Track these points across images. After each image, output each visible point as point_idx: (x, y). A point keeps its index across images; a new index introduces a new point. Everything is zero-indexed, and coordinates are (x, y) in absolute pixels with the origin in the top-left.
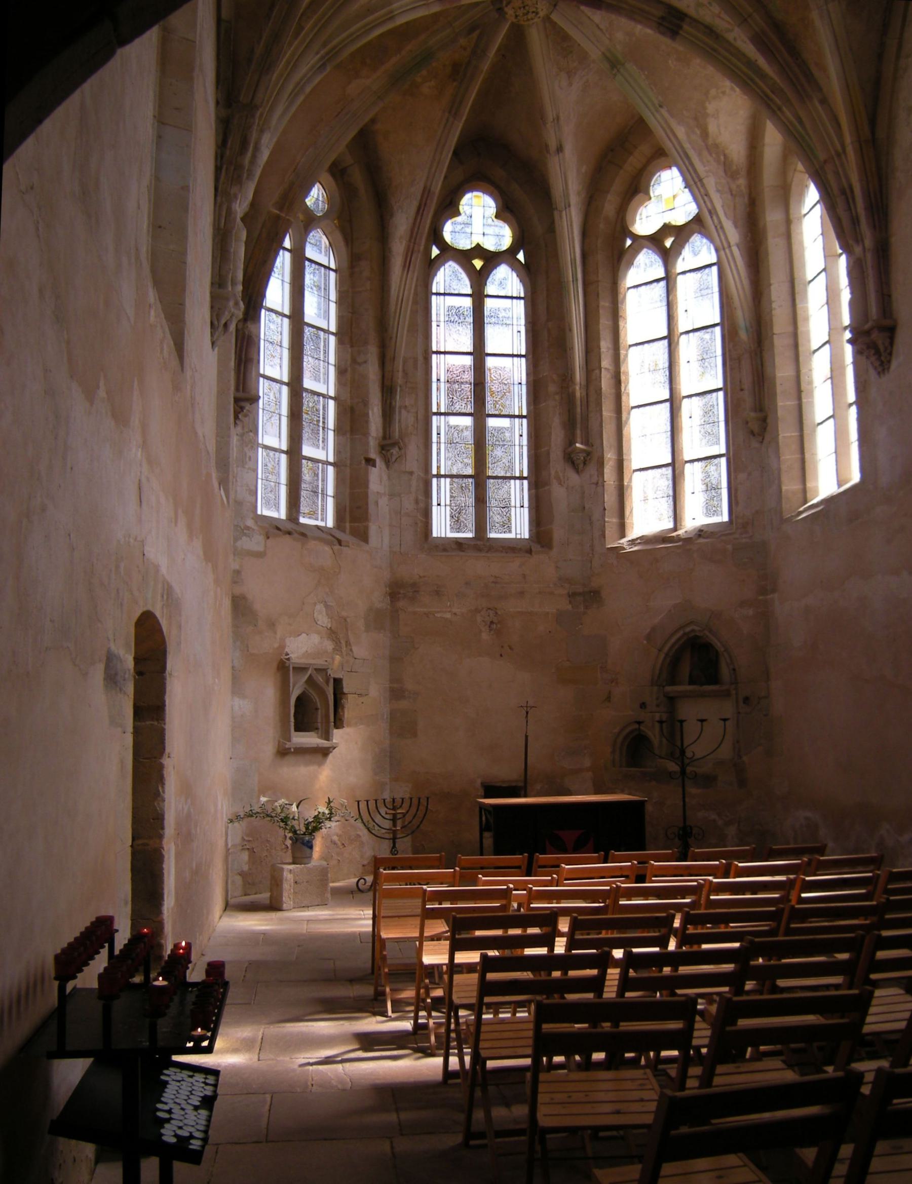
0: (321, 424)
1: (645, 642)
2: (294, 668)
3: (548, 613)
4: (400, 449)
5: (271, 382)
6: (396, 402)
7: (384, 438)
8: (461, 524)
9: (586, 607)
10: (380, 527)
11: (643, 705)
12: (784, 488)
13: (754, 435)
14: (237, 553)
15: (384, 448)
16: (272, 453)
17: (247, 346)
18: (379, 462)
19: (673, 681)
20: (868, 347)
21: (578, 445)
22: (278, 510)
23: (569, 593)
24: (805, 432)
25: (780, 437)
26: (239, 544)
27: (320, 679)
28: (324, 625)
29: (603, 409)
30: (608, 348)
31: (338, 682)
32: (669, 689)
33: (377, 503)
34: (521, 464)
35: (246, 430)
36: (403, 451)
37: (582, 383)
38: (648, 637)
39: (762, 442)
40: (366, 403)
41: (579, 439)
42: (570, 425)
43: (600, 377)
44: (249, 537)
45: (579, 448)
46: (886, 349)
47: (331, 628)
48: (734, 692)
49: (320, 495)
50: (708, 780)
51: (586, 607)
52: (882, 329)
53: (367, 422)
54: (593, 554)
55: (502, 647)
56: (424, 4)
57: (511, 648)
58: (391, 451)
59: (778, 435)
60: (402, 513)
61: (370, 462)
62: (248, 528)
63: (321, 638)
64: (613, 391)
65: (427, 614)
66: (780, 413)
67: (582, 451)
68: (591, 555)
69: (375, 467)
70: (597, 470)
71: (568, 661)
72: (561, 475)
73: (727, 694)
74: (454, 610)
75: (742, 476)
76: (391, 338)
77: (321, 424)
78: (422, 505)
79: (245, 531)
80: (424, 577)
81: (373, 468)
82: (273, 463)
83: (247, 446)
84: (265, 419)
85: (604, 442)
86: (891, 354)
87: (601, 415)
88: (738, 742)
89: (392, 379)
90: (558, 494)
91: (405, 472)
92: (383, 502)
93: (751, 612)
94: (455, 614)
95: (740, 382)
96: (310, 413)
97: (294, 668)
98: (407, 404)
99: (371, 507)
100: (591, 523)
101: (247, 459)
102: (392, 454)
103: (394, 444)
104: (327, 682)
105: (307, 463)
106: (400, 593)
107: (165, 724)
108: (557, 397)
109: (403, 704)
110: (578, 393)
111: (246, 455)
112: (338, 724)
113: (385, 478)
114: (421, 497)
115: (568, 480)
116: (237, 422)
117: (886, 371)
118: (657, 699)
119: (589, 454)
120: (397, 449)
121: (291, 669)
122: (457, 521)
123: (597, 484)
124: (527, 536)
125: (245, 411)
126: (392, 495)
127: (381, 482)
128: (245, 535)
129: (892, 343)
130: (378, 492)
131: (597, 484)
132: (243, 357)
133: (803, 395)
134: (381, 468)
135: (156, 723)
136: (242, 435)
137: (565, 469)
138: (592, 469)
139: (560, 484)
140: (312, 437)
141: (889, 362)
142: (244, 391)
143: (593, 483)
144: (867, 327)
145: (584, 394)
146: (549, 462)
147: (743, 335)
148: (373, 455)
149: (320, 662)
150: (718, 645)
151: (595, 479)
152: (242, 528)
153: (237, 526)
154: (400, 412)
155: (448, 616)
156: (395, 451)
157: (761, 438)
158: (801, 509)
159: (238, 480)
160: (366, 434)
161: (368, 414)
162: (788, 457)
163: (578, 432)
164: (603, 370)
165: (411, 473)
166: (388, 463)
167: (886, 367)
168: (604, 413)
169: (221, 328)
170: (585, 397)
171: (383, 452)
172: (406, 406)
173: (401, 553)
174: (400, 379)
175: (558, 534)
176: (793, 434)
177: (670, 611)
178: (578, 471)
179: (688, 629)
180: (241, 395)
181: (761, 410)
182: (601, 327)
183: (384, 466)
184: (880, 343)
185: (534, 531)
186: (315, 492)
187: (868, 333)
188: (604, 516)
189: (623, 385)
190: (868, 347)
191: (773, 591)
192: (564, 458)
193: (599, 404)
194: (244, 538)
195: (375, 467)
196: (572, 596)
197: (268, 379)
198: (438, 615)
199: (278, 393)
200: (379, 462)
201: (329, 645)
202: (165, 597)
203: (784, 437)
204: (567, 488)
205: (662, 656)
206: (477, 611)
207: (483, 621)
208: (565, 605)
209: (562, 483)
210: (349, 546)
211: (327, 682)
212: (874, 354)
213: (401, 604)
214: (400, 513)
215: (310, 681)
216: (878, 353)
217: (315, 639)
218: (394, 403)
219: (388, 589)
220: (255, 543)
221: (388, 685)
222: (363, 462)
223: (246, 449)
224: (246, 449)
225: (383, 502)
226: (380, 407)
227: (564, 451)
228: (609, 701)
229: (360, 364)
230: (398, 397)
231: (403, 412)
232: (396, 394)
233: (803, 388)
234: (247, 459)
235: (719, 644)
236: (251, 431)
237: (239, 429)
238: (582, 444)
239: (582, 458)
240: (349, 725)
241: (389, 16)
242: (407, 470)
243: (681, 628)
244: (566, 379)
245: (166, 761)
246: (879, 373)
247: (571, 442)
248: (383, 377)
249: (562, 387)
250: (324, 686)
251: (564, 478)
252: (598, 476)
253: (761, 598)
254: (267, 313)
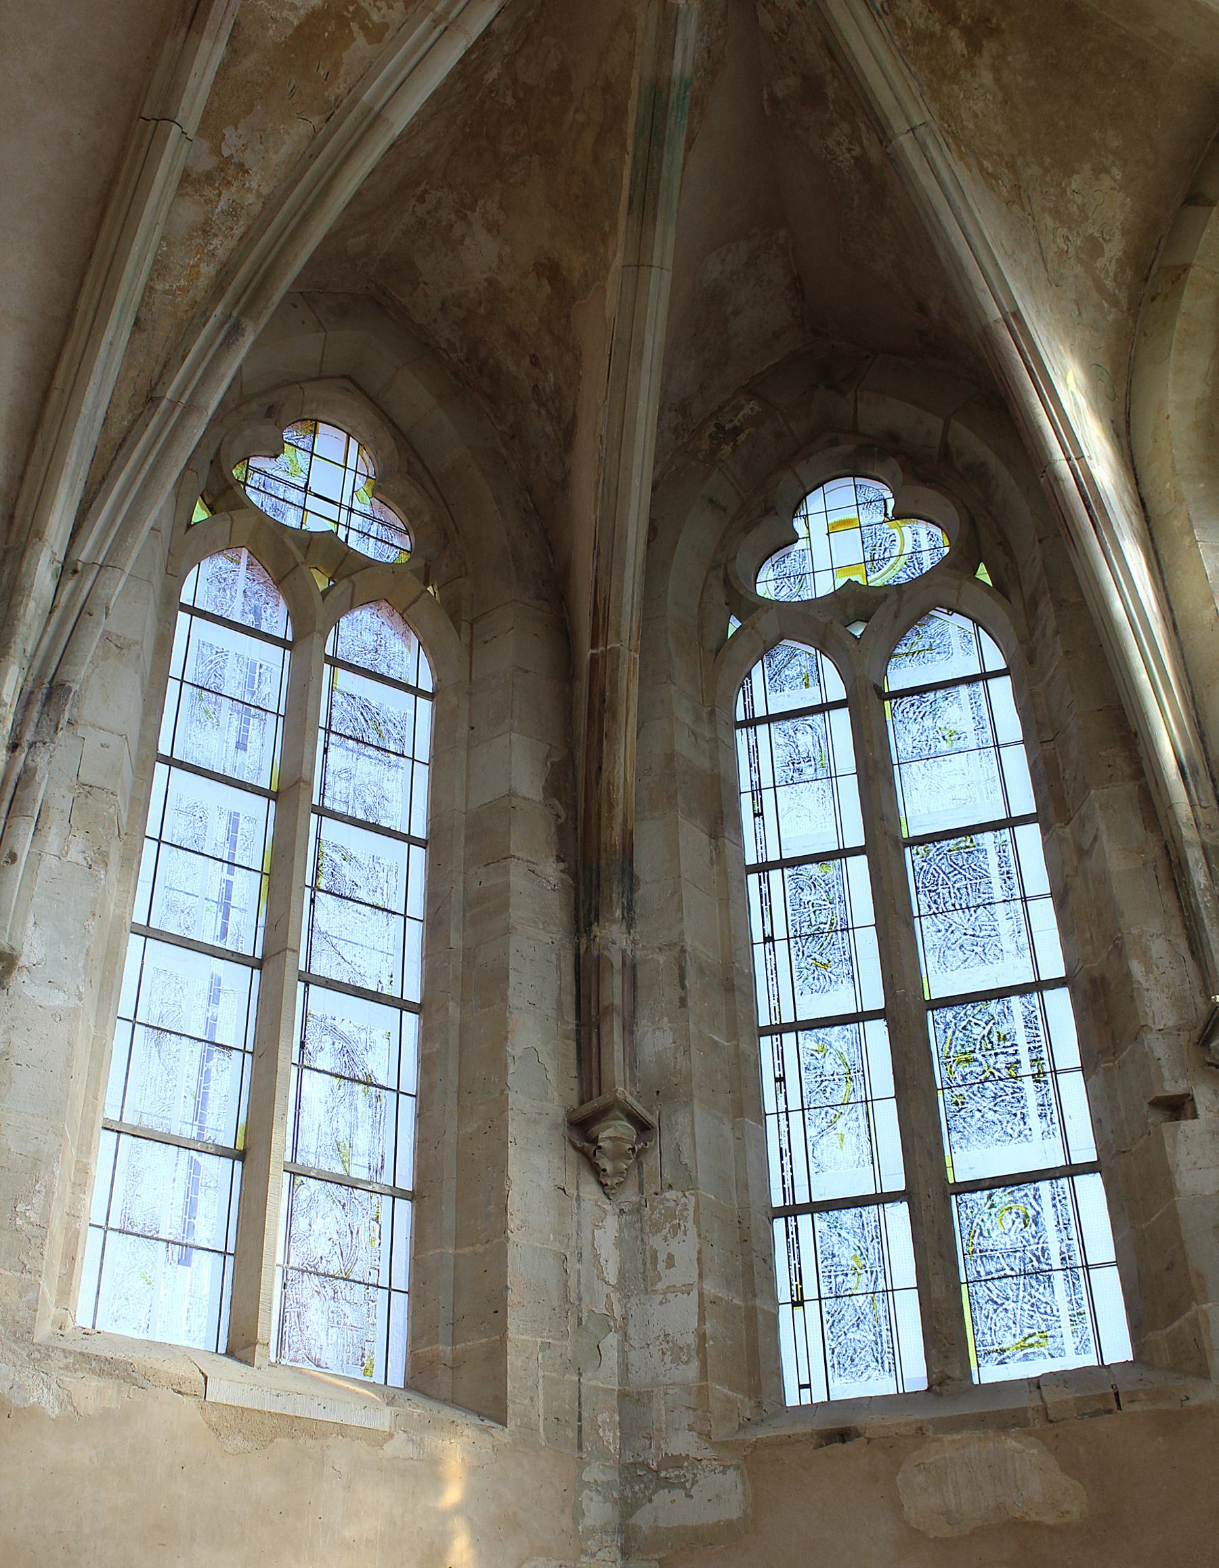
0: (1026, 1069)
5: (821, 1033)
16: (847, 1217)
18: (1203, 1096)
22: (895, 1367)
26: (643, 1519)
35: (650, 1189)
44: (682, 1486)
49: (1058, 1277)
56: (446, 29)
62: (676, 1461)
77: (1026, 1069)
79: (663, 1474)
82: (854, 1242)
83: (659, 1231)
84: (811, 1132)
96: (978, 1055)
105: (990, 1197)
128: (667, 1484)
140: (995, 1117)
152: (654, 1467)
159: (631, 1331)
197: (810, 1029)
199: (854, 1050)
223: (655, 1241)
224: (655, 1241)
234: (661, 1266)
236: (670, 1187)
237: (629, 1195)
241: (370, 118)
254: (787, 872)
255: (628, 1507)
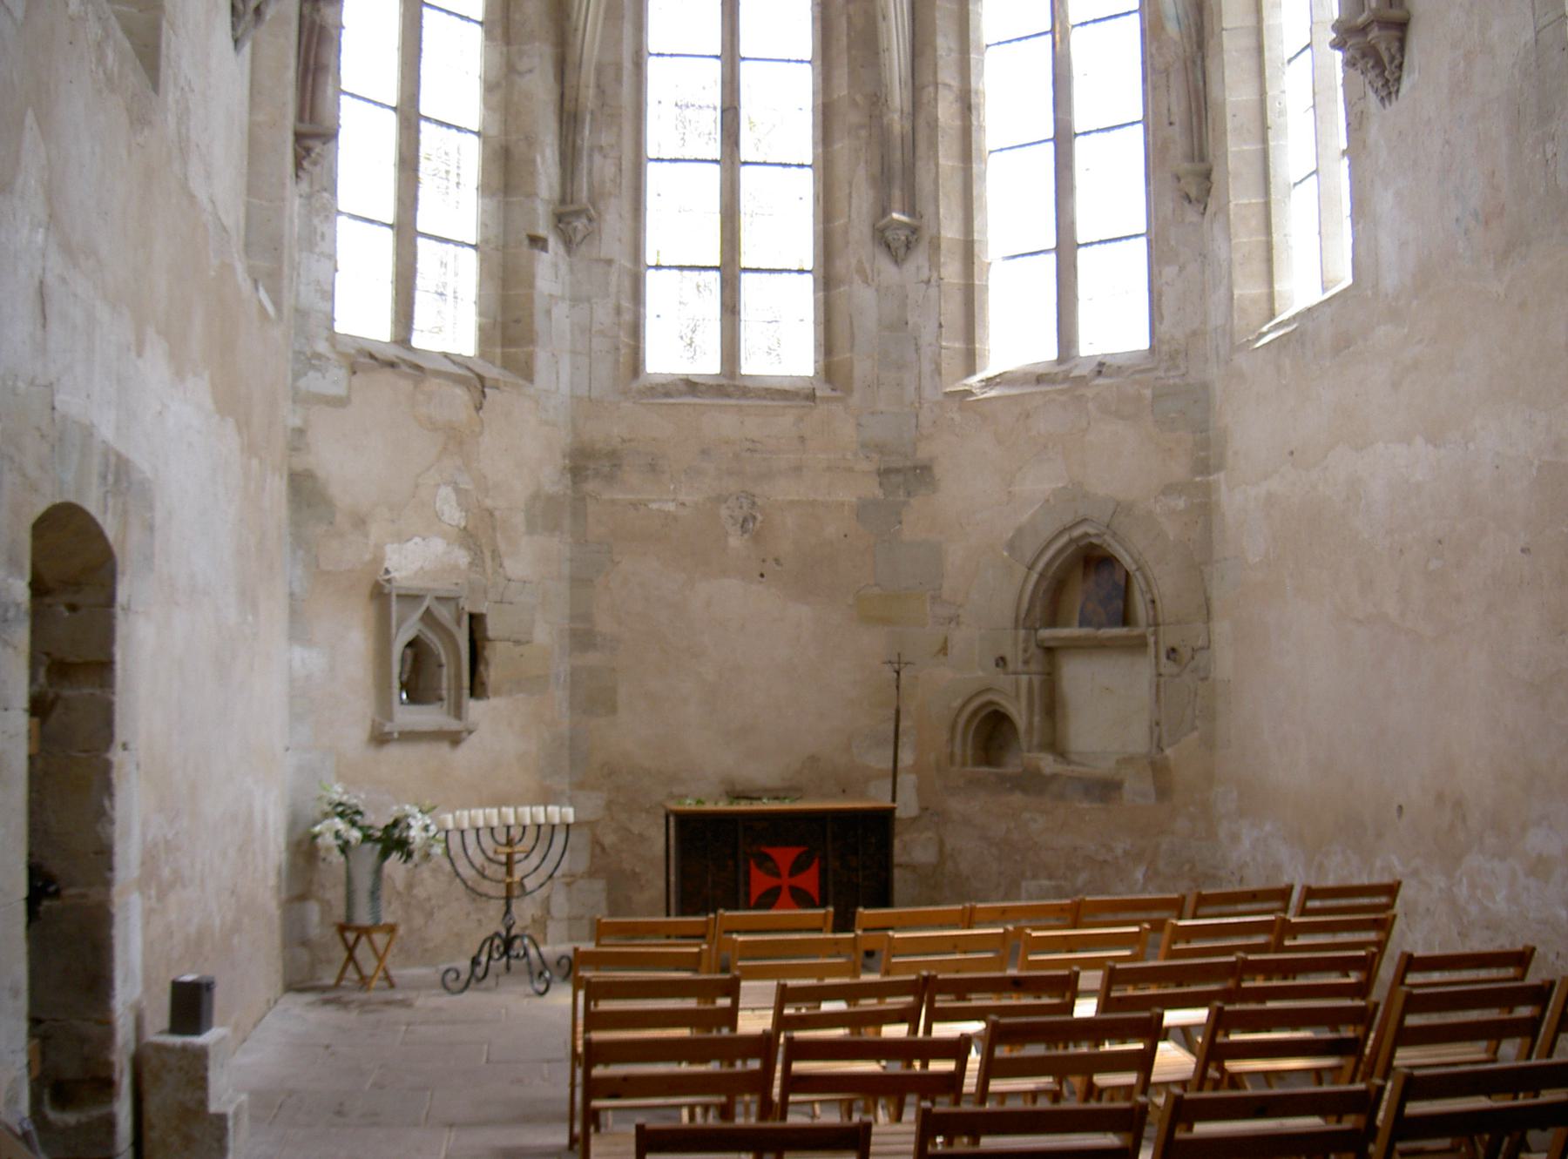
1: (1006, 554)
2: (399, 596)
3: (843, 504)
4: (590, 220)
6: (583, 140)
7: (563, 201)
8: (695, 351)
9: (909, 494)
10: (553, 355)
11: (1001, 661)
12: (1237, 292)
13: (1190, 202)
14: (302, 399)
15: (561, 219)
17: (319, 44)
19: (1053, 620)
20: (1364, 56)
21: (895, 215)
23: (879, 469)
24: (1273, 197)
25: (1232, 205)
27: (444, 614)
28: (453, 523)
29: (940, 154)
30: (950, 49)
31: (476, 621)
32: (1045, 633)
33: (548, 312)
34: (801, 248)
35: (317, 187)
36: (595, 225)
37: (905, 109)
38: (1011, 546)
39: (1203, 214)
40: (530, 141)
41: (897, 204)
42: (883, 180)
43: (936, 100)
45: (898, 221)
46: (1392, 59)
47: (465, 528)
48: (1151, 640)
50: (1105, 789)
51: (909, 494)
52: (1386, 24)
53: (533, 173)
54: (920, 403)
55: (764, 561)
57: (777, 561)
58: (575, 224)
59: (1229, 202)
60: (593, 332)
61: (537, 242)
62: (319, 356)
63: (448, 544)
64: (958, 123)
65: (635, 505)
66: (1232, 164)
67: (902, 225)
68: (917, 405)
69: (546, 251)
70: (929, 260)
71: (876, 585)
72: (867, 266)
73: (1137, 646)
74: (682, 497)
75: (1170, 272)
76: (576, 30)
78: (627, 317)
79: (313, 362)
80: (630, 440)
81: (544, 254)
85: (941, 211)
86: (1400, 66)
87: (937, 165)
88: (1158, 724)
89: (577, 100)
90: (862, 298)
91: (598, 260)
92: (561, 311)
93: (1181, 504)
94: (683, 504)
95: (1169, 110)
97: (399, 596)
98: (603, 143)
99: (540, 322)
100: (917, 349)
101: (318, 238)
102: (575, 229)
103: (577, 214)
104: (459, 623)
106: (587, 469)
107: (113, 693)
108: (863, 133)
109: (593, 658)
110: (897, 122)
111: (315, 228)
112: (477, 688)
113: (564, 269)
114: (626, 304)
115: (879, 275)
116: (300, 174)
117: (1393, 96)
118: (1025, 651)
119: (915, 230)
120: (584, 221)
121: (394, 598)
122: (690, 345)
123: (928, 282)
124: (810, 372)
125: (313, 155)
126: (575, 300)
127: (557, 278)
128: (313, 367)
129: (1402, 49)
130: (551, 296)
131: (928, 282)
132: (312, 62)
133: (1271, 133)
134: (556, 254)
135: (98, 692)
136: (309, 197)
137: (874, 257)
138: (919, 258)
139: (866, 281)
141: (1398, 80)
142: (312, 120)
143: (922, 282)
144: (1361, 19)
145: (908, 126)
146: (847, 243)
147: (1172, 29)
148: (543, 230)
149: (444, 586)
150: (1127, 561)
151: (925, 274)
153: (300, 352)
154: (590, 156)
155: (671, 507)
156: (580, 224)
157: (1202, 207)
158: (1265, 329)
159: (302, 272)
160: (532, 195)
161: (534, 161)
162: (1245, 240)
163: (897, 193)
164: (940, 86)
165: (609, 262)
166: (568, 243)
167: (1393, 89)
168: (942, 161)
169: (249, 16)
170: (911, 132)
171: (560, 225)
172: (601, 148)
173: (591, 400)
174: (589, 96)
175: (862, 368)
176: (1254, 201)
177: (1048, 501)
178: (897, 261)
179: (1077, 533)
180: (306, 128)
181: (1202, 159)
182: (938, 15)
183: (561, 250)
184: (1382, 47)
185: (821, 363)
186: (441, 294)
187: (1364, 30)
188: (939, 336)
189: (974, 112)
190: (1364, 56)
191: (1219, 468)
192: (873, 237)
193: (933, 145)
194: (311, 374)
195: (546, 251)
196: (884, 473)
198: (654, 506)
200: (553, 242)
201: (462, 558)
202: (111, 478)
203: (1236, 205)
204: (877, 290)
205: (1034, 576)
206: (720, 499)
207: (731, 517)
208: (872, 489)
209: (869, 281)
210: (498, 388)
211: (459, 623)
212: (1373, 67)
213: (590, 486)
214: (590, 330)
215: (429, 617)
216: (1379, 64)
217: (438, 546)
218: (579, 142)
219: (567, 462)
220: (333, 381)
221: (567, 626)
222: (526, 242)
223: (316, 221)
225: (561, 311)
226: (556, 147)
227: (874, 226)
228: (945, 654)
229: (520, 74)
230: (587, 132)
231: (597, 158)
232: (583, 128)
233: (1270, 122)
234: (318, 238)
235: (1128, 558)
236: (325, 190)
237: (304, 186)
238: (904, 213)
239: (903, 238)
240: (498, 693)
242: (602, 255)
243: (1065, 530)
244: (876, 101)
245: (116, 755)
246: (1382, 99)
247: (885, 211)
248: (562, 96)
249: (871, 117)
250: (451, 625)
251: (873, 271)
252: (930, 270)
253: (1198, 479)
255: (297, 376)
